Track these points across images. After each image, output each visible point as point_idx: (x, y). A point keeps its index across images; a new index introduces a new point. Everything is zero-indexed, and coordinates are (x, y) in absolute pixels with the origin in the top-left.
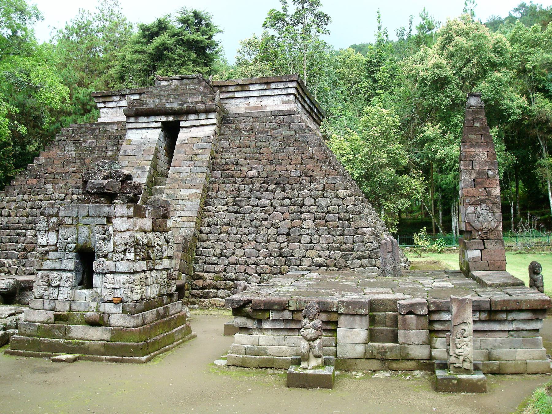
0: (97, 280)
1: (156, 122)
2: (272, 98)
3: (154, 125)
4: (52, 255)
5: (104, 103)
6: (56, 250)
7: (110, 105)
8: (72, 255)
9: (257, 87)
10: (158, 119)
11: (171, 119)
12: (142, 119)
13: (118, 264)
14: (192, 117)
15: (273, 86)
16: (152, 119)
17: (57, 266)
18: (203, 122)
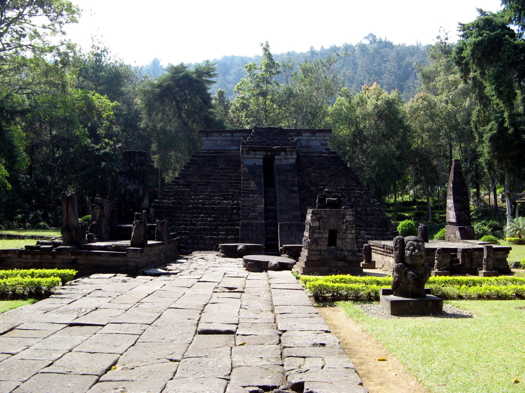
0: (339, 242)
1: (260, 155)
2: (315, 142)
3: (258, 156)
4: (317, 231)
5: (207, 136)
6: (319, 229)
7: (211, 138)
8: (327, 231)
9: (308, 134)
10: (262, 153)
11: (269, 153)
12: (251, 152)
13: (349, 235)
14: (283, 153)
15: (317, 134)
16: (258, 153)
17: (320, 236)
18: (289, 157)
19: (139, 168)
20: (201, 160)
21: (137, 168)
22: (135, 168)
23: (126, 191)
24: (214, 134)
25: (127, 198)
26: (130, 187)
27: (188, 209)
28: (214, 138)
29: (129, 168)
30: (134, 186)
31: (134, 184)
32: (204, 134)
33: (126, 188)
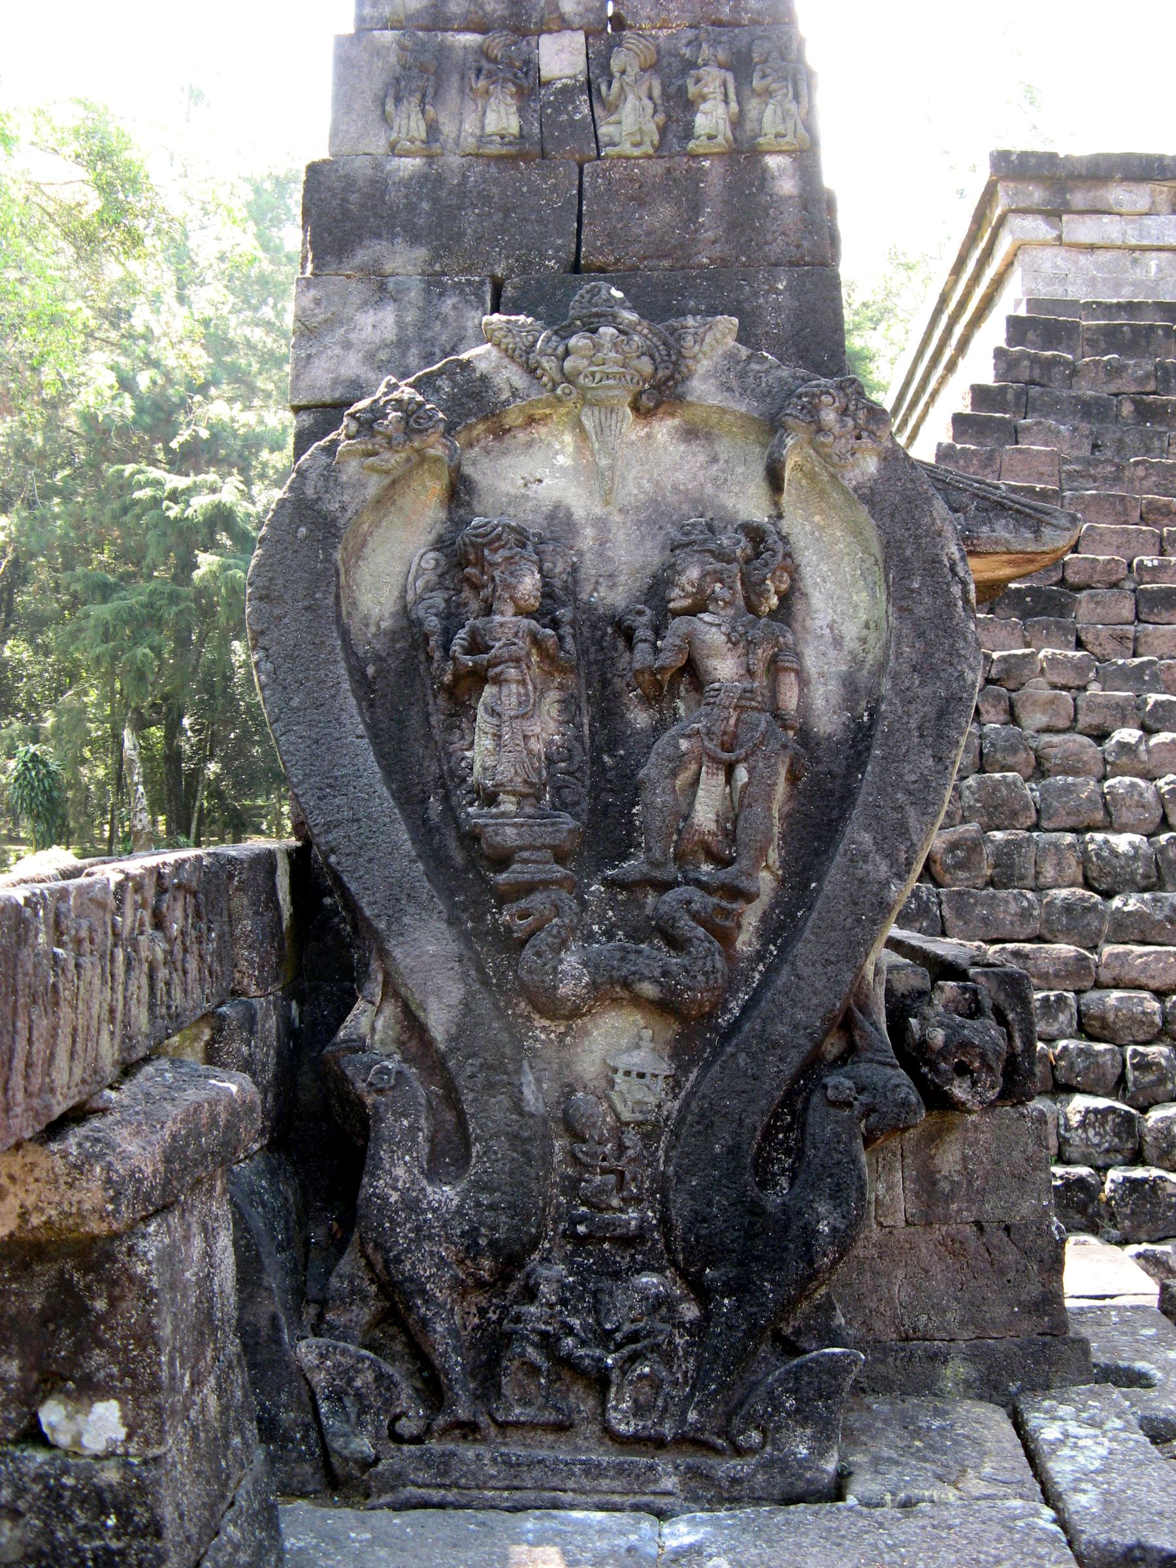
5: (1053, 213)
7: (1084, 230)
19: (711, 119)
20: (1114, 371)
21: (678, 106)
22: (630, 124)
23: (464, 558)
24: (1118, 194)
25: (513, 736)
26: (543, 474)
27: (1102, 878)
28: (1107, 229)
29: (502, 117)
30: (659, 460)
31: (660, 395)
32: (1036, 194)
33: (459, 491)
